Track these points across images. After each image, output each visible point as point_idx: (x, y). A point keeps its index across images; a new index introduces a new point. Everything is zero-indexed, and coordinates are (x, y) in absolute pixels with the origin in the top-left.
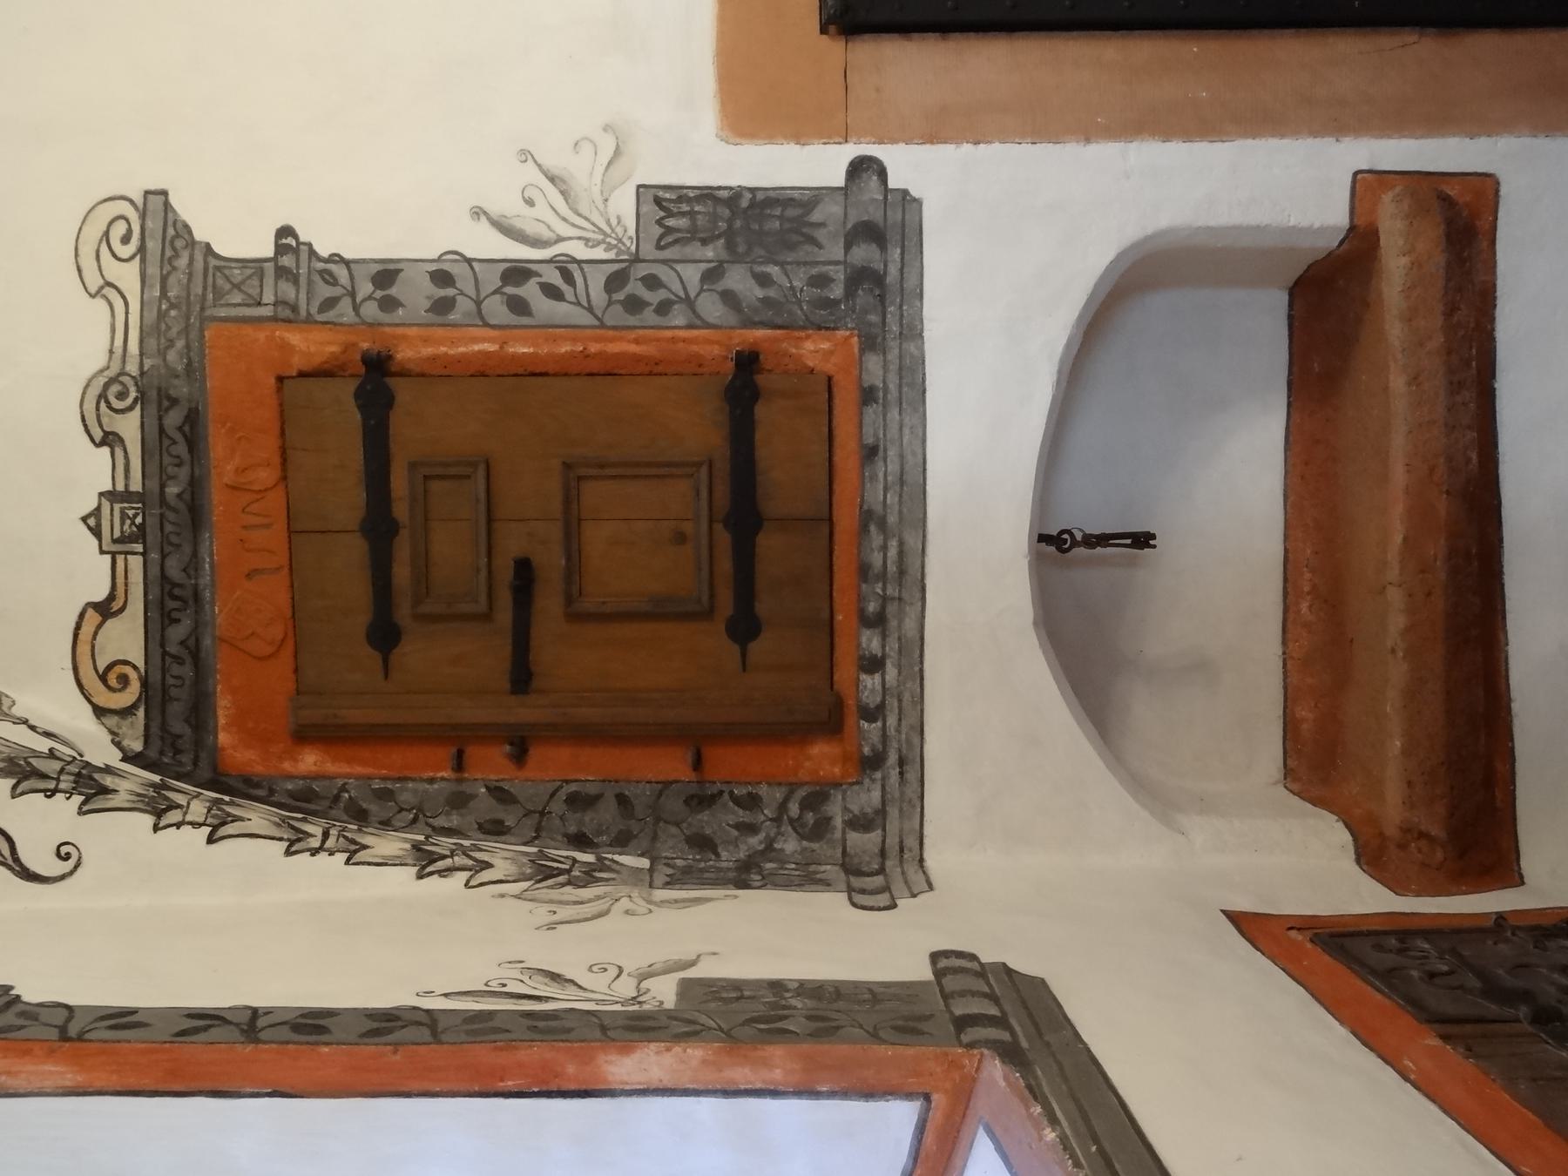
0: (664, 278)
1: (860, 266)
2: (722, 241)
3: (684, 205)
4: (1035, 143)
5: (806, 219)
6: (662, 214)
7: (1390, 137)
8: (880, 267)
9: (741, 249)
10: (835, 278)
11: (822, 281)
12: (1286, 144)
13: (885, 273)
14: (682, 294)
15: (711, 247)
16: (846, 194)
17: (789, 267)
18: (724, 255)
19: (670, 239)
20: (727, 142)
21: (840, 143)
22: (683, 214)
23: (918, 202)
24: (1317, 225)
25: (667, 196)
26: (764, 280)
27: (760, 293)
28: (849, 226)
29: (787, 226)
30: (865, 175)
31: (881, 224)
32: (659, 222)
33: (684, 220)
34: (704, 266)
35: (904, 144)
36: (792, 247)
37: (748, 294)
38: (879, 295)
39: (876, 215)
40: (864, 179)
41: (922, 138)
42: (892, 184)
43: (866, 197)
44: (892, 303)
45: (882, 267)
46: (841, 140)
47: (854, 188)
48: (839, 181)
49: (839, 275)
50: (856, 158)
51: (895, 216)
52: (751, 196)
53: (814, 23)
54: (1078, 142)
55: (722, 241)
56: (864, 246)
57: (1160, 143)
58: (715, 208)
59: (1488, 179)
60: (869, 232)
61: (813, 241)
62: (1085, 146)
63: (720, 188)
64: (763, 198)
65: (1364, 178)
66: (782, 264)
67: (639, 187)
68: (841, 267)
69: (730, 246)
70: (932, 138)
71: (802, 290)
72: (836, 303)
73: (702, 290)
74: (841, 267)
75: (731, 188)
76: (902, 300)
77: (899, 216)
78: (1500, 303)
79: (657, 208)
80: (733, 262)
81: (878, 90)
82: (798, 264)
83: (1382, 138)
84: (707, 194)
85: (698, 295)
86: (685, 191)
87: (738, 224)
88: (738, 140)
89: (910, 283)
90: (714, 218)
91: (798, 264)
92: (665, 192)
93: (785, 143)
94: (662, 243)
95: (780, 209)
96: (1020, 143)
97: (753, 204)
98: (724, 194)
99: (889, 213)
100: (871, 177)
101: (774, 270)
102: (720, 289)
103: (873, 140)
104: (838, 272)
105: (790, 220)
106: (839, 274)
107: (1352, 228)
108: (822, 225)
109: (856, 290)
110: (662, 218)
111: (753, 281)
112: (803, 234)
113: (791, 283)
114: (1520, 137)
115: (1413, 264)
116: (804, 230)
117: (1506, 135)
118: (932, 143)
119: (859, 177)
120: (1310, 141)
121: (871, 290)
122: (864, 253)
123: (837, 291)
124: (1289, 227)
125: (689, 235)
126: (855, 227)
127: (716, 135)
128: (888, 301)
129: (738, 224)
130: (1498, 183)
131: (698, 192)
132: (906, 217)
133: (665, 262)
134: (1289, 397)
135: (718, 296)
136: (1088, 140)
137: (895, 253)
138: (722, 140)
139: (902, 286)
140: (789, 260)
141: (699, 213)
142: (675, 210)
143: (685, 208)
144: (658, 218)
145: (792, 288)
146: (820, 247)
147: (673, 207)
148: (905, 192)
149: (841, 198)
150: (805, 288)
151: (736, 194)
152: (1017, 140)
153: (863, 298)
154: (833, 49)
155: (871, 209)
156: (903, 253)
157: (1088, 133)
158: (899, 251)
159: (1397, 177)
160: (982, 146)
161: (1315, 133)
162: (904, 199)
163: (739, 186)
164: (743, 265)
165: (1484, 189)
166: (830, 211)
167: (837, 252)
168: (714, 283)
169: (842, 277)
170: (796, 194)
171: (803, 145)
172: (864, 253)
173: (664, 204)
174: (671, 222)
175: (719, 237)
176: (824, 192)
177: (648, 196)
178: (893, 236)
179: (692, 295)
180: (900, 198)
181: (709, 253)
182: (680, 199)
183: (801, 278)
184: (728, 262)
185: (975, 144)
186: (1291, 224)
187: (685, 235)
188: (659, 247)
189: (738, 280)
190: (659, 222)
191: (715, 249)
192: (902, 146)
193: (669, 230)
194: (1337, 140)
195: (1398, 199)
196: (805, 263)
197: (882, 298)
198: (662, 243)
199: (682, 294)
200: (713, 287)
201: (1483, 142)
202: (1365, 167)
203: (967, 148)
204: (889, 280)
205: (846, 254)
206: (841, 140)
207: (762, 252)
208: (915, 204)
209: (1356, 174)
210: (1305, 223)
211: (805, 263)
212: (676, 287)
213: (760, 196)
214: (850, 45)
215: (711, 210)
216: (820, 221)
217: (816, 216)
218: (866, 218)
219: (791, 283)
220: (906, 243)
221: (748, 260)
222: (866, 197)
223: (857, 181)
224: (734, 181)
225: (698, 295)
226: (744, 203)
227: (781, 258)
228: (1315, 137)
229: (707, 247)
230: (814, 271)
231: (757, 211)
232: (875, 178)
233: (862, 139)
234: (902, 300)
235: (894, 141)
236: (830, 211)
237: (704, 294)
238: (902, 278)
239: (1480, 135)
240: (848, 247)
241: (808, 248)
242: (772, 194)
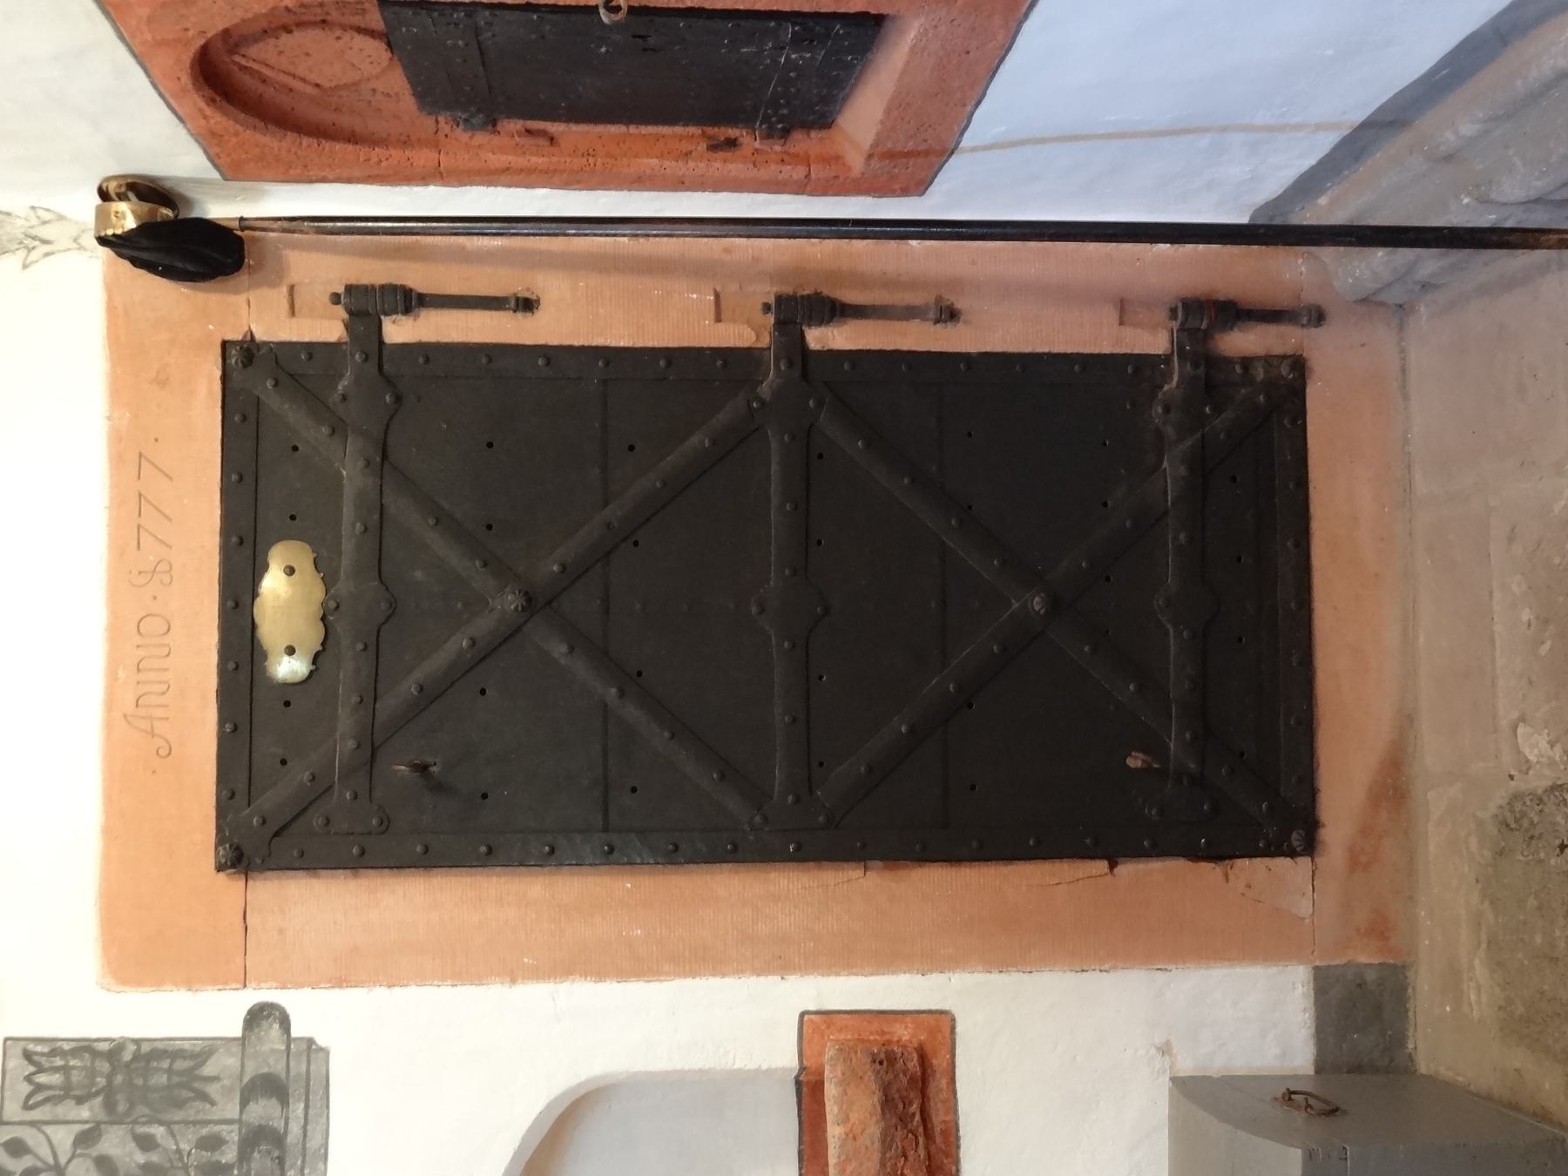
0: (30, 1142)
1: (257, 1124)
2: (100, 1099)
3: (58, 1058)
4: (456, 985)
5: (197, 1072)
6: (32, 1069)
7: (838, 974)
8: (279, 1124)
9: (122, 1107)
10: (227, 1138)
11: (213, 1143)
12: (729, 982)
13: (286, 1132)
14: (51, 1161)
15: (87, 1105)
16: (243, 1045)
17: (176, 1128)
18: (102, 1116)
19: (39, 1097)
20: (108, 990)
21: (238, 989)
22: (56, 1070)
23: (325, 1052)
24: (764, 1067)
25: (39, 1049)
26: (146, 1143)
27: (141, 1158)
28: (246, 1079)
29: (176, 1079)
30: (265, 1024)
31: (283, 1076)
32: (28, 1079)
33: (58, 1076)
34: (78, 1128)
35: (310, 989)
36: (180, 1104)
37: (127, 1159)
38: (278, 1158)
39: (278, 1067)
40: (264, 1028)
41: (330, 982)
42: (295, 1033)
43: (266, 1048)
44: (292, 1166)
45: (283, 1124)
46: (238, 986)
47: (253, 1037)
48: (237, 1031)
49: (232, 1135)
50: (254, 1006)
51: (298, 1067)
52: (135, 1047)
53: (210, 861)
54: (502, 983)
55: (100, 1099)
56: (263, 1102)
57: (592, 984)
58: (93, 1062)
59: (942, 1016)
60: (271, 1087)
61: (205, 1097)
62: (511, 987)
63: (98, 1040)
64: (148, 1049)
65: (811, 1021)
66: (168, 1124)
67: (6, 1040)
68: (235, 1127)
69: (109, 1106)
70: (340, 982)
71: (189, 1154)
72: (229, 1167)
73: (73, 1157)
74: (235, 1127)
75: (113, 1040)
76: (304, 1162)
77: (304, 1068)
78: (964, 1143)
79: (26, 1062)
80: (112, 1123)
81: (281, 931)
82: (186, 1123)
83: (829, 975)
84: (85, 1047)
85: (69, 1161)
86: (59, 1043)
87: (119, 1079)
88: (121, 988)
89: (314, 1143)
90: (92, 1073)
91: (186, 1123)
92: (36, 1045)
93: (174, 988)
94: (31, 1102)
95: (169, 1061)
96: (439, 986)
97: (137, 1057)
98: (104, 1046)
99: (292, 1064)
100: (271, 1026)
101: (158, 1131)
102: (94, 1154)
103: (275, 985)
104: (232, 1131)
105: (180, 1073)
106: (233, 1134)
107: (802, 1069)
108: (215, 1079)
109: (253, 1152)
110: (34, 1074)
111: (134, 1144)
112: (192, 1090)
113: (177, 1145)
114: (973, 972)
115: (847, 1135)
116: (196, 1085)
117: (958, 971)
118: (341, 987)
119: (259, 1025)
120: (753, 979)
121: (269, 1152)
122: (263, 1110)
123: (229, 1155)
124: (734, 1070)
125: (62, 1093)
126: (252, 1081)
127: (97, 983)
128: (288, 1164)
129: (119, 1079)
130: (953, 1020)
131: (73, 1044)
132: (312, 1067)
133: (32, 1124)
134: (800, 1169)
135: (90, 1164)
136: (513, 981)
137: (298, 1109)
138: (103, 988)
139: (304, 1148)
140: (177, 1118)
141: (74, 1068)
142: (47, 1065)
143: (59, 1062)
144: (27, 1073)
145: (179, 1151)
146: (213, 1103)
147: (43, 1060)
148: (310, 1041)
149: (236, 1049)
150: (193, 1151)
151: (118, 1046)
152: (436, 983)
153: (259, 1161)
154: (230, 887)
155: (271, 1061)
156: (307, 1107)
157: (513, 976)
158: (302, 1105)
159: (848, 1016)
160: (397, 989)
161: (759, 972)
162: (309, 1048)
163: (122, 1037)
164: (123, 1126)
165: (940, 1025)
166: (223, 1064)
167: (231, 1109)
168: (87, 1148)
169: (236, 1138)
170: (187, 1045)
171: (196, 990)
172: (263, 1110)
173: (36, 1058)
174: (42, 1079)
175: (97, 1094)
176: (219, 1042)
177: (17, 1050)
178: (296, 1090)
179: (63, 1160)
180: (305, 1047)
181: (85, 1113)
182: (53, 1053)
183: (189, 1140)
184: (105, 1123)
185: (389, 987)
186: (736, 1067)
187: (57, 1093)
188: (27, 1107)
189: (115, 1144)
190: (28, 1079)
191: (91, 1109)
192: (307, 991)
193: (39, 1088)
194: (782, 978)
195: (833, 1062)
196: (194, 1123)
197: (281, 1161)
198: (31, 1102)
199: (51, 1161)
200: (87, 1152)
201: (936, 979)
202: (812, 1008)
203: (380, 992)
204: (290, 1139)
205: (241, 1112)
206: (238, 986)
207: (146, 1111)
208: (321, 1055)
209: (803, 1015)
210: (752, 1066)
211: (194, 1123)
212: (45, 1152)
213: (145, 1048)
214: (250, 883)
215: (89, 1064)
216: (212, 1074)
217: (208, 1070)
218: (265, 1070)
219: (177, 1145)
220: (311, 1097)
221: (129, 1120)
222: (266, 1048)
223: (256, 1030)
224: (116, 1033)
225: (69, 1161)
226: (127, 1056)
227: (166, 1117)
228: (759, 975)
229: (82, 1106)
230: (205, 1131)
231: (142, 1064)
232: (276, 1026)
233: (263, 985)
234: (304, 1162)
235: (299, 985)
236: (223, 1064)
237: (75, 1161)
238: (305, 1135)
239: (932, 972)
240: (244, 1103)
241: (199, 1105)
242: (159, 1045)
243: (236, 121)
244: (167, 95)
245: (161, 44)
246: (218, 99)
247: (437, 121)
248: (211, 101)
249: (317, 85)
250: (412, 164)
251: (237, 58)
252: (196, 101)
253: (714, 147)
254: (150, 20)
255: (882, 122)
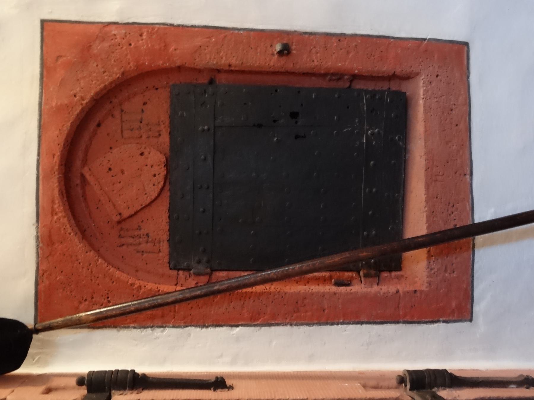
243: (69, 221)
244: (41, 177)
245: (59, 109)
246: (65, 199)
247: (178, 274)
248: (61, 192)
249: (120, 214)
250: (159, 290)
251: (86, 171)
252: (55, 184)
253: (339, 284)
254: (62, 82)
255: (427, 201)
